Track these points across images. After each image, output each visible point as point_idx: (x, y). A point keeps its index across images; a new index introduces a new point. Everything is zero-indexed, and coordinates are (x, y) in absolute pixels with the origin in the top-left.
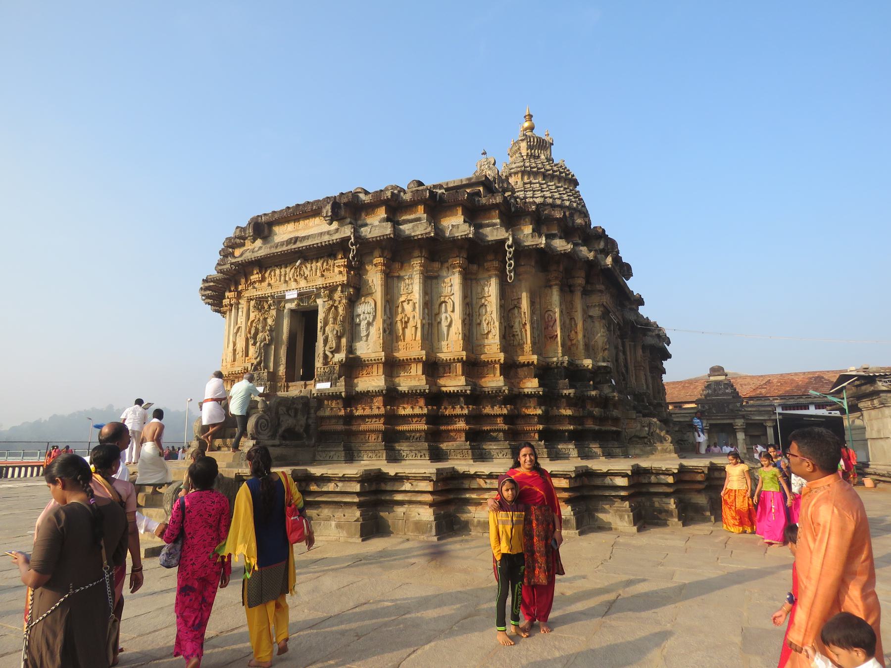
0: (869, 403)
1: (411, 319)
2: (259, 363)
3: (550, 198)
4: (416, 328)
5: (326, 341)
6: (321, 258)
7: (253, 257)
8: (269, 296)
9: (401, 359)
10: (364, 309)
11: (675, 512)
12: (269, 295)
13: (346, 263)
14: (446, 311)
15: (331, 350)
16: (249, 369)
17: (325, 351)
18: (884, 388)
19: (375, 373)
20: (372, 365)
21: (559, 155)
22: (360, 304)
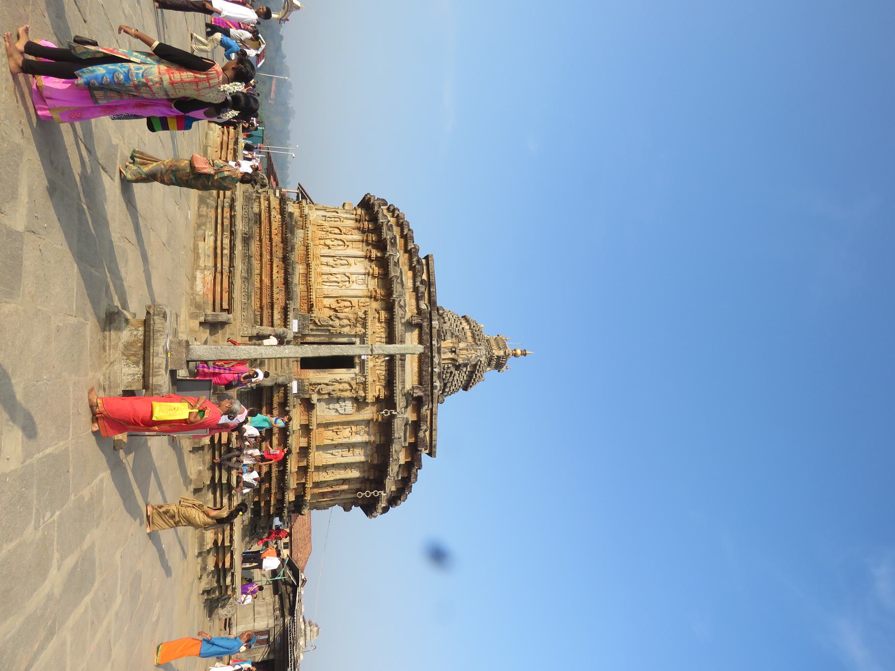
0: (278, 606)
1: (338, 436)
2: (315, 324)
3: (453, 380)
4: (332, 440)
5: (327, 384)
6: (388, 374)
7: (396, 323)
8: (366, 331)
9: (311, 433)
10: (349, 406)
11: (210, 597)
12: (367, 333)
13: (381, 398)
14: (342, 451)
15: (320, 390)
16: (312, 315)
17: (320, 384)
18: (286, 621)
19: (302, 418)
20: (309, 416)
21: (490, 374)
22: (352, 402)
